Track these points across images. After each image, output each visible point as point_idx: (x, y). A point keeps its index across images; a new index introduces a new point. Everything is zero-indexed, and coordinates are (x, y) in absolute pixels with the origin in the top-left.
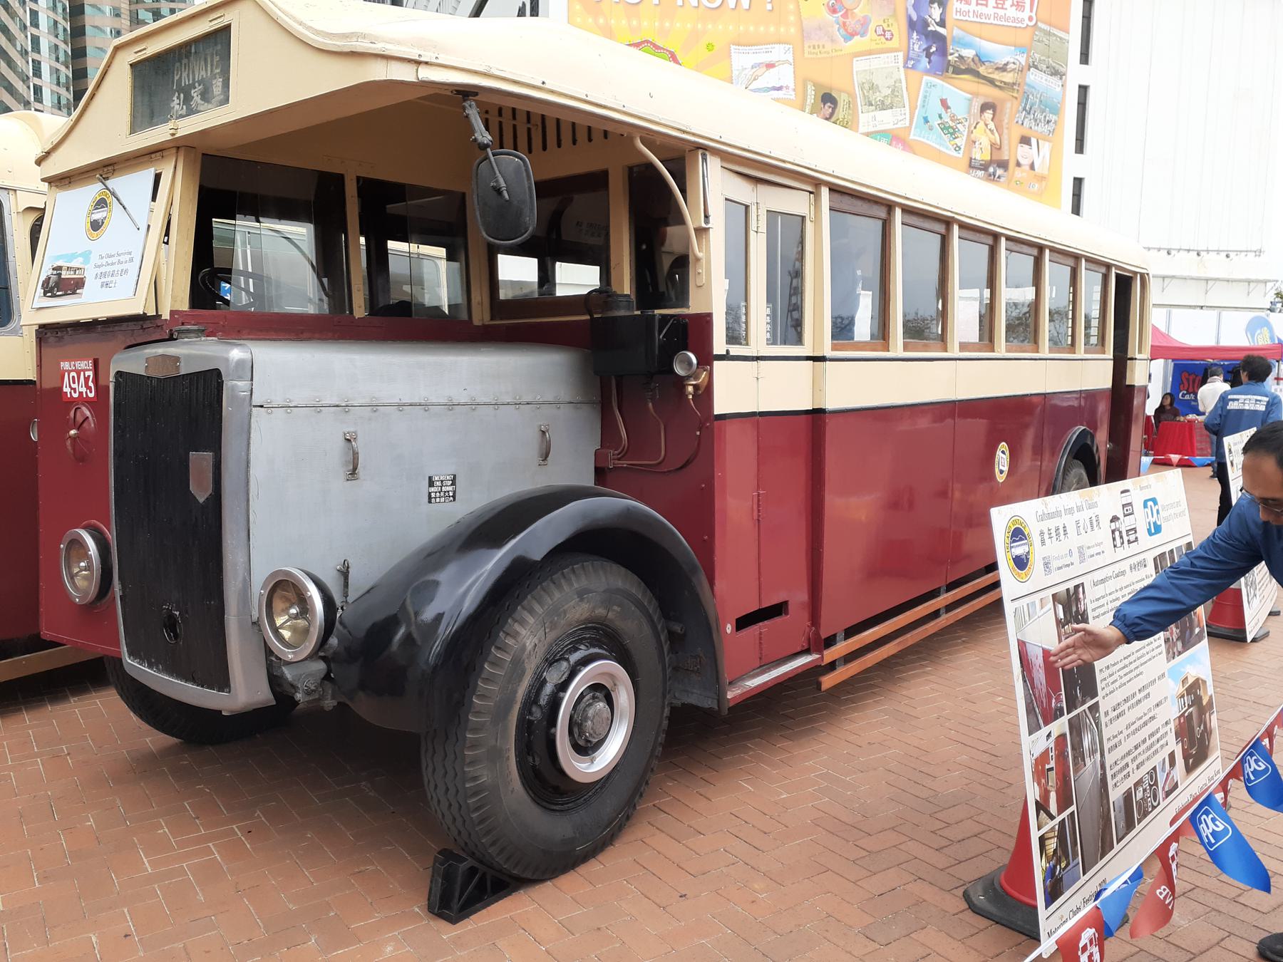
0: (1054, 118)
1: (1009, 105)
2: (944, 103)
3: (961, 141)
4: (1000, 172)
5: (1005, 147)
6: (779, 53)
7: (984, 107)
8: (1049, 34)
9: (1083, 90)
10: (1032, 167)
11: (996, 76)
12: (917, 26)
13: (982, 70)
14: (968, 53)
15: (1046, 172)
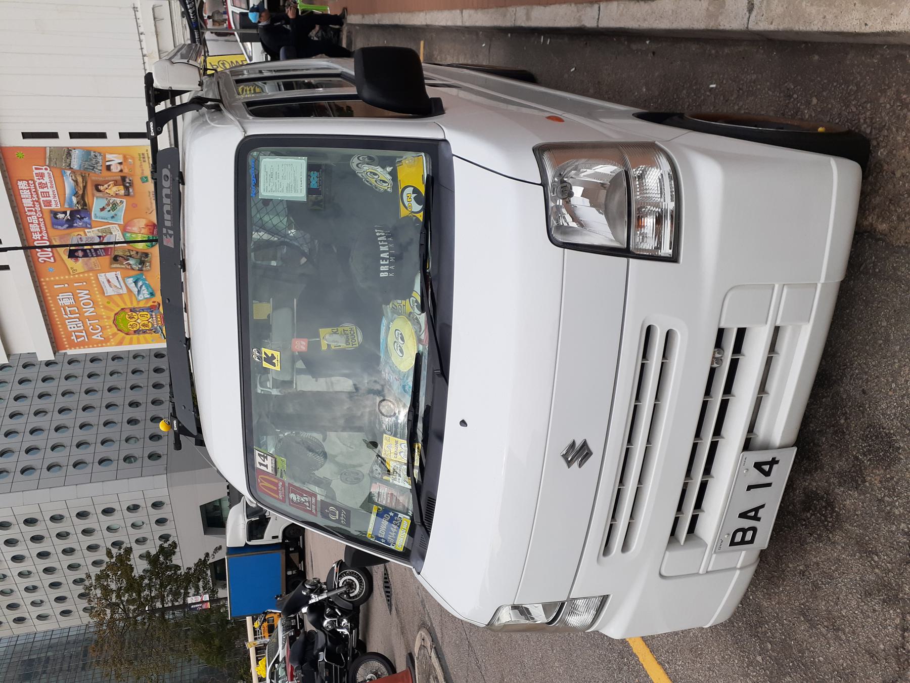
0: (92, 154)
1: (93, 178)
2: (103, 209)
3: (118, 200)
4: (128, 181)
5: (115, 178)
6: (102, 278)
7: (99, 191)
8: (50, 159)
9: (73, 135)
10: (120, 163)
11: (81, 185)
12: (70, 223)
13: (81, 192)
14: (74, 200)
15: (121, 156)
